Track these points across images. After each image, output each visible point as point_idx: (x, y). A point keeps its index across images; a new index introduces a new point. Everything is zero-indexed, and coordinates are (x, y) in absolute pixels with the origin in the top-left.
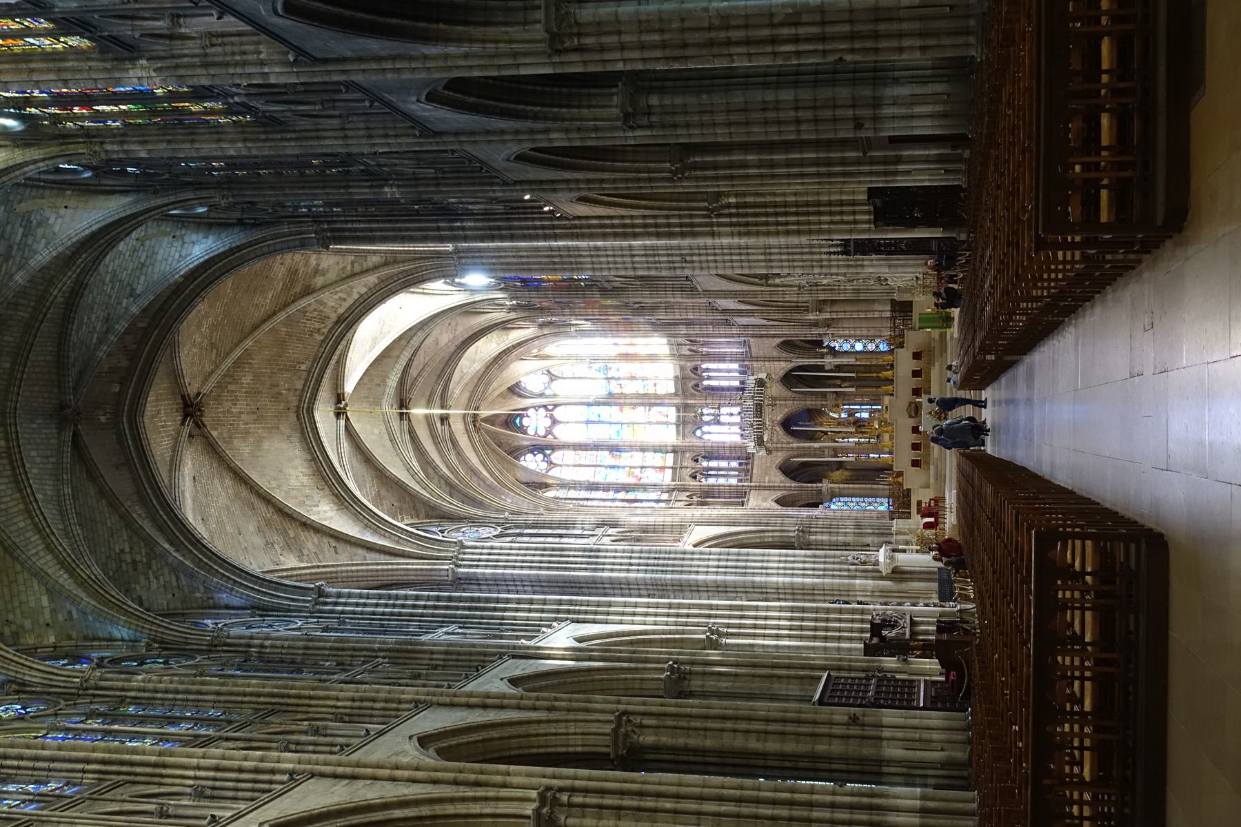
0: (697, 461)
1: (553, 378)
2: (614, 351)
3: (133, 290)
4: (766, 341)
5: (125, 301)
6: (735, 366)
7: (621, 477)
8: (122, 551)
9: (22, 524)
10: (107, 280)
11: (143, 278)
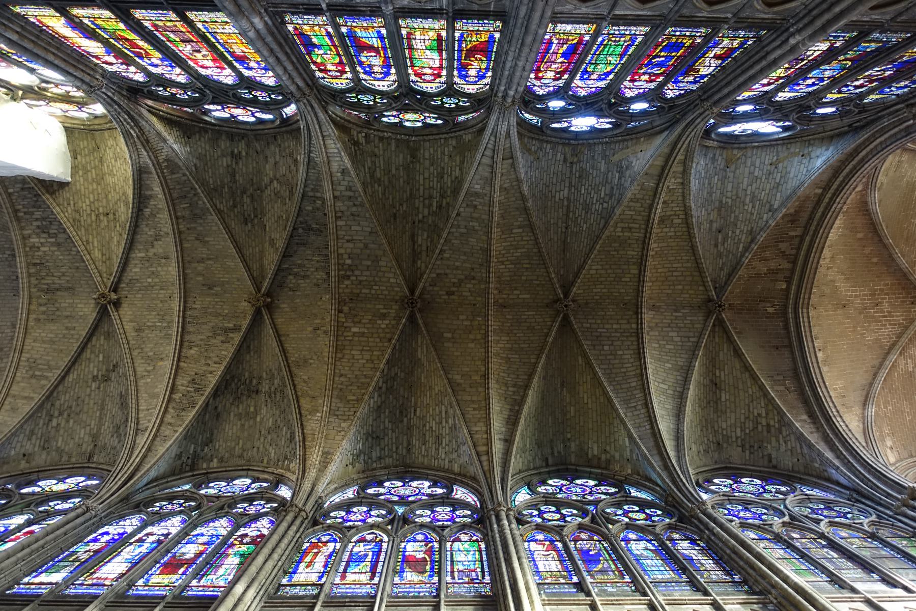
3: (771, 206)
5: (765, 216)
8: (759, 415)
9: (634, 384)
10: (748, 200)
11: (779, 194)
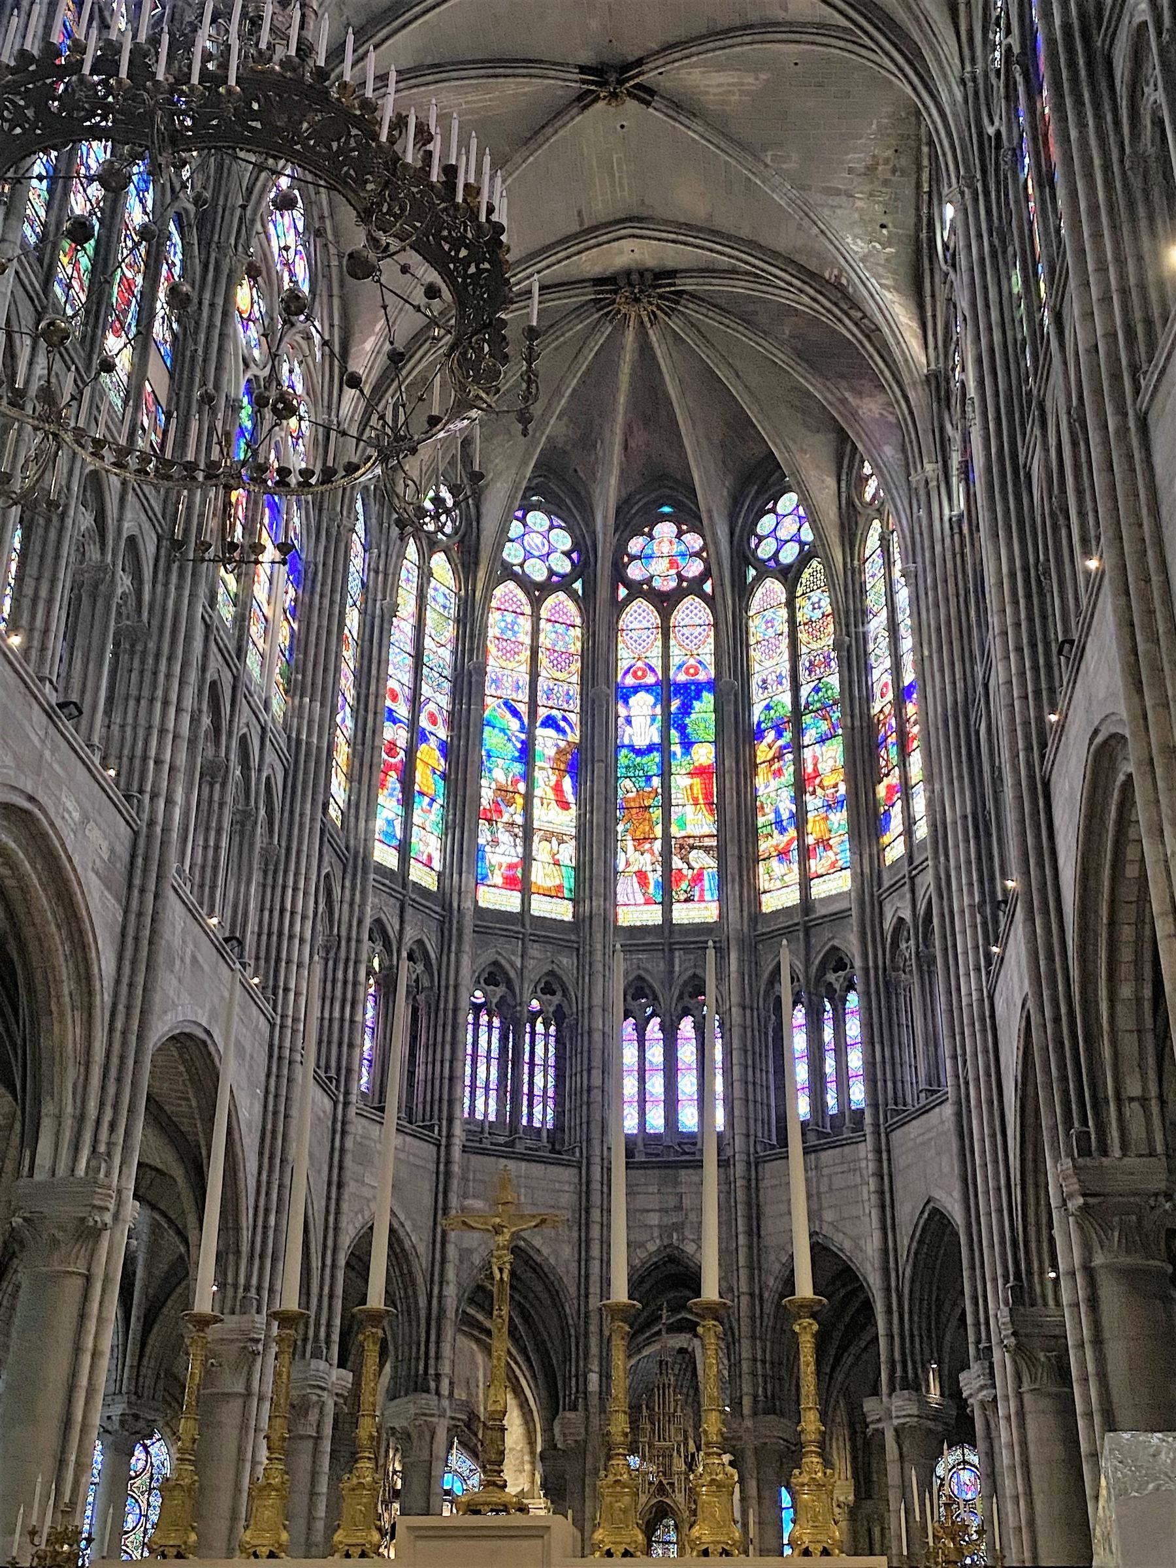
0: (548, 990)
1: (790, 576)
2: (881, 704)
4: (949, 1165)
6: (858, 1093)
7: (500, 771)
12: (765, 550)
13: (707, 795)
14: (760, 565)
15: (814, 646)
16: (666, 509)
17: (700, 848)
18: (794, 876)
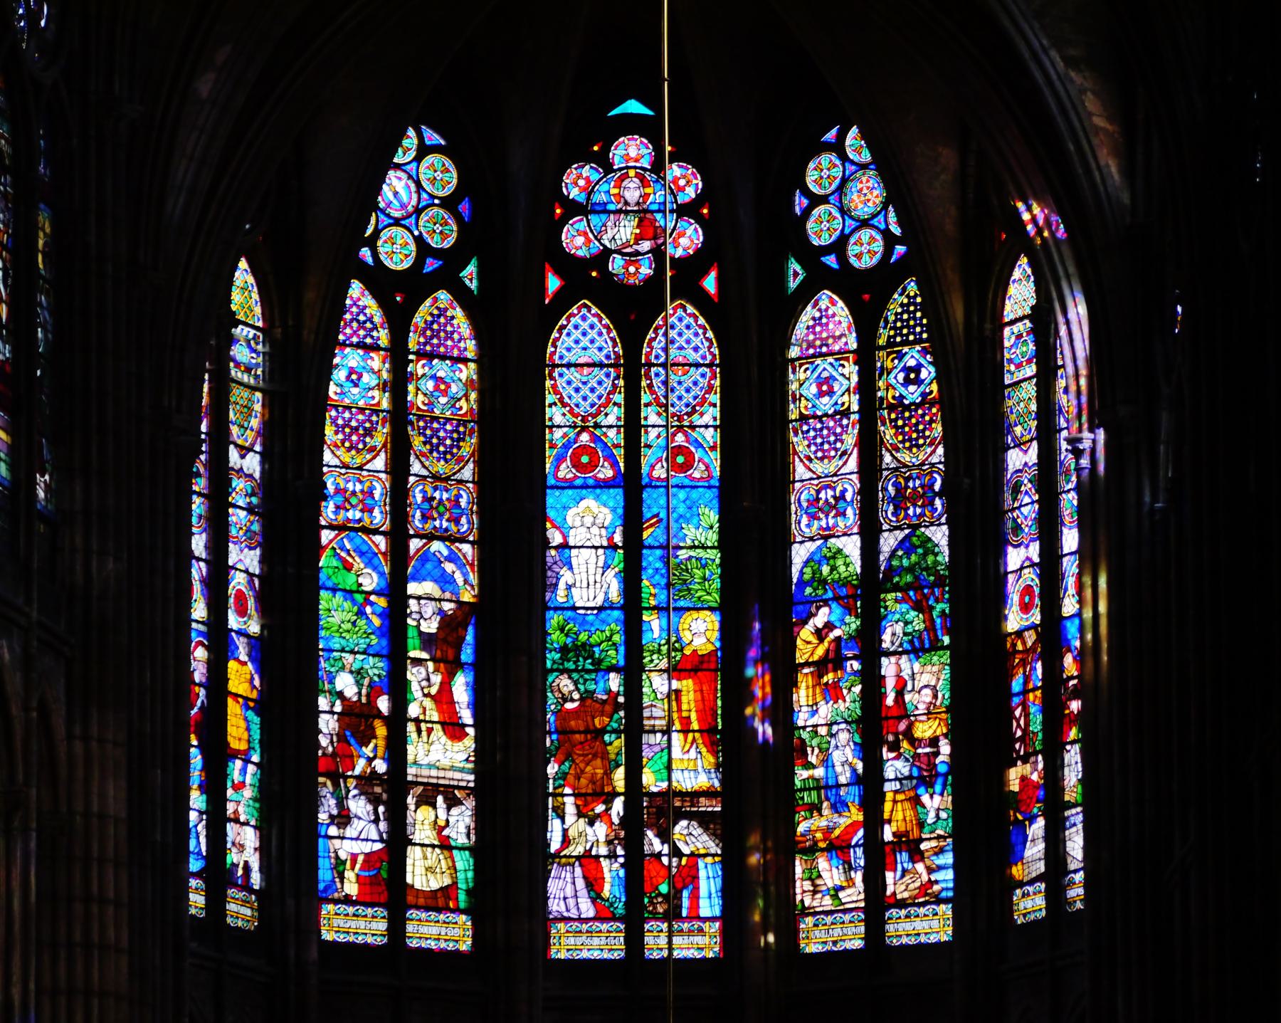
12: (821, 228)
13: (706, 711)
14: (811, 256)
15: (906, 457)
16: (633, 107)
17: (690, 816)
18: (854, 895)
